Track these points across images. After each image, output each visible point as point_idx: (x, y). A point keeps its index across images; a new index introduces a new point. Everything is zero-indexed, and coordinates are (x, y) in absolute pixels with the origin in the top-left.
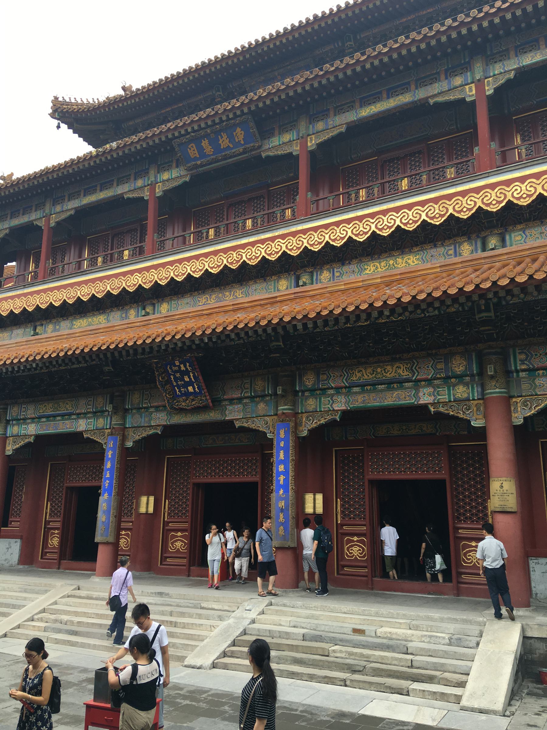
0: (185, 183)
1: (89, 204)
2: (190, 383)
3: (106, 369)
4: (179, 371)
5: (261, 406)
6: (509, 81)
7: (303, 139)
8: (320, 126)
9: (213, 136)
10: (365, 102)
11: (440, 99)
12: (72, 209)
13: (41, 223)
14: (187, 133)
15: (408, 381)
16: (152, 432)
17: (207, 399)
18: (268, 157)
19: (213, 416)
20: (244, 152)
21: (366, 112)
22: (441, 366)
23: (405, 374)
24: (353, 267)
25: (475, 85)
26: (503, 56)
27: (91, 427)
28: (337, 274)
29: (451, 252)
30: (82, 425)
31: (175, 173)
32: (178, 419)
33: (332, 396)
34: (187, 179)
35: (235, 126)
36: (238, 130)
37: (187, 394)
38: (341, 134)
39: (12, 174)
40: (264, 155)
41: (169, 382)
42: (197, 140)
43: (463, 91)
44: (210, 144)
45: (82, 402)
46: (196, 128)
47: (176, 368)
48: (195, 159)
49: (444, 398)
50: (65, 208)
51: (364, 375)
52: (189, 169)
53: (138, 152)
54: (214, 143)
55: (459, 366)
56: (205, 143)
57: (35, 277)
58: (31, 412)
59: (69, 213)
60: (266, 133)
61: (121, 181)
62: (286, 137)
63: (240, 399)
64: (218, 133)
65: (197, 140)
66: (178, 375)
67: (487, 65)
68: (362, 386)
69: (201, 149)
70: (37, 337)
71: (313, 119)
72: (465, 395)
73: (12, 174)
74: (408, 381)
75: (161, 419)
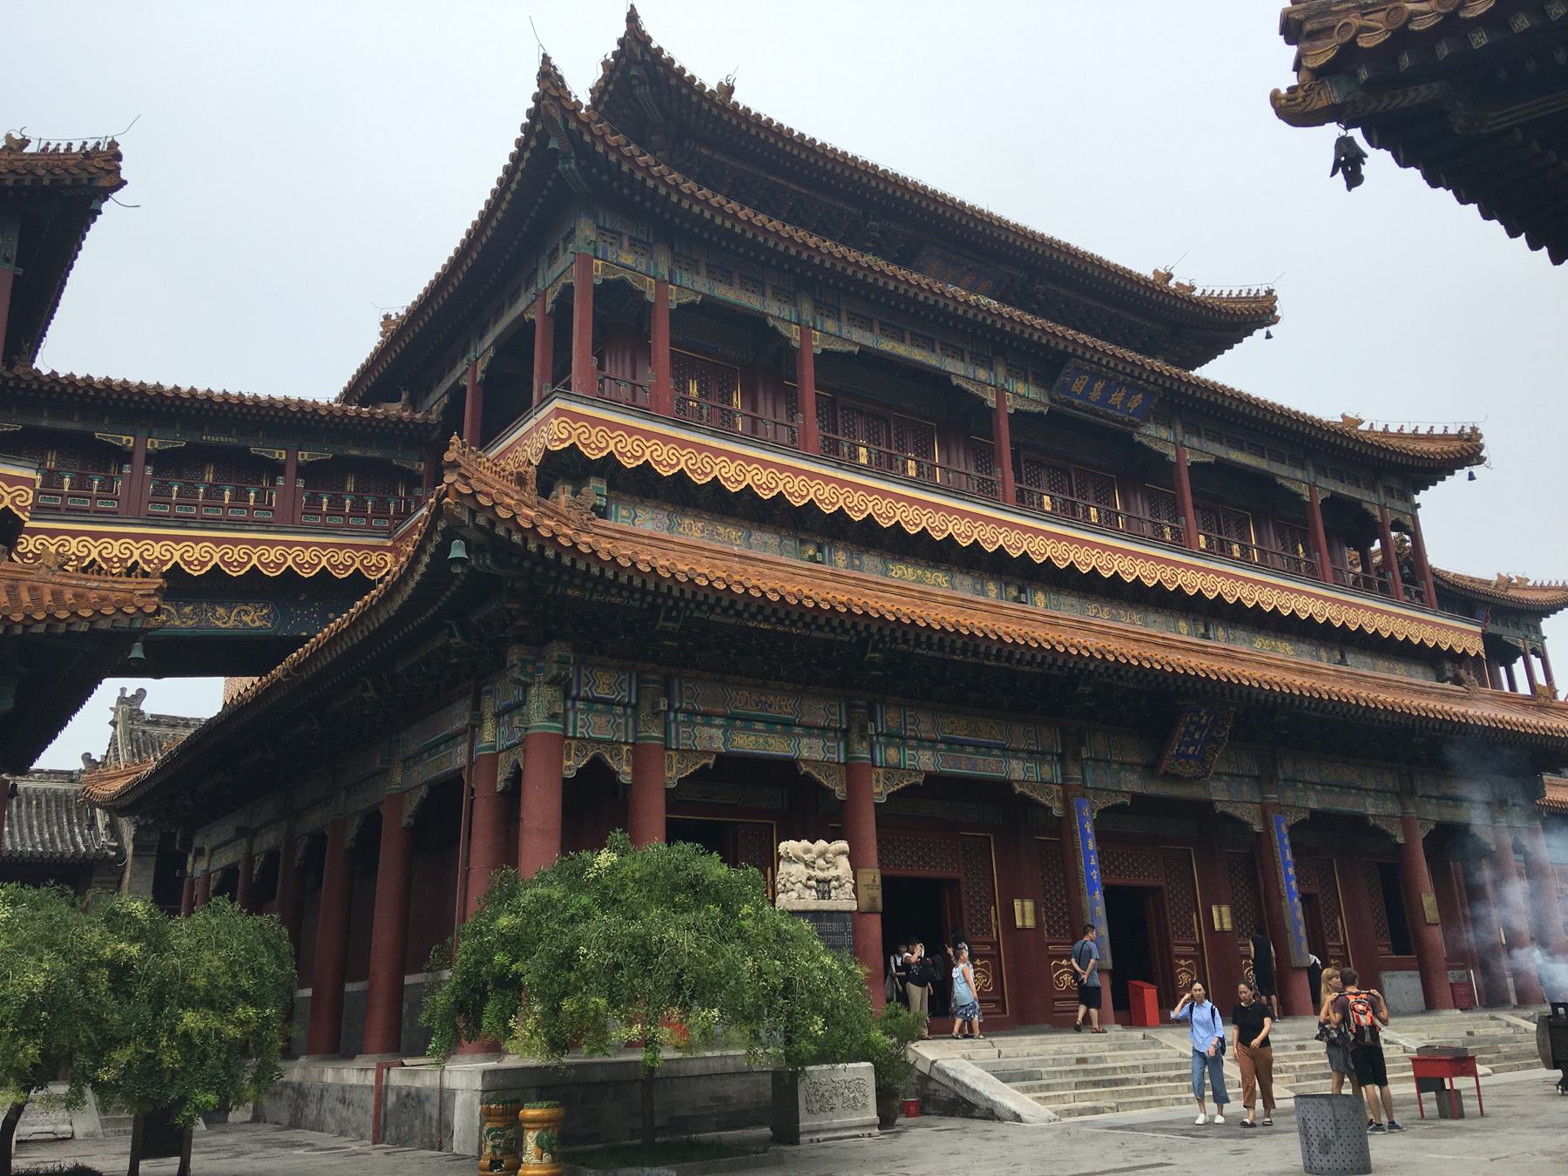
1: (890, 354)
12: (856, 344)
20: (1127, 424)
27: (1033, 776)
30: (1017, 770)
31: (1033, 392)
35: (1142, 389)
40: (1137, 438)
46: (1112, 365)
50: (845, 335)
53: (1038, 344)
54: (1108, 392)
56: (1099, 385)
59: (849, 348)
60: (1146, 415)
61: (958, 354)
62: (1164, 433)
64: (1120, 385)
65: (1095, 376)
69: (1089, 387)
70: (1205, 642)
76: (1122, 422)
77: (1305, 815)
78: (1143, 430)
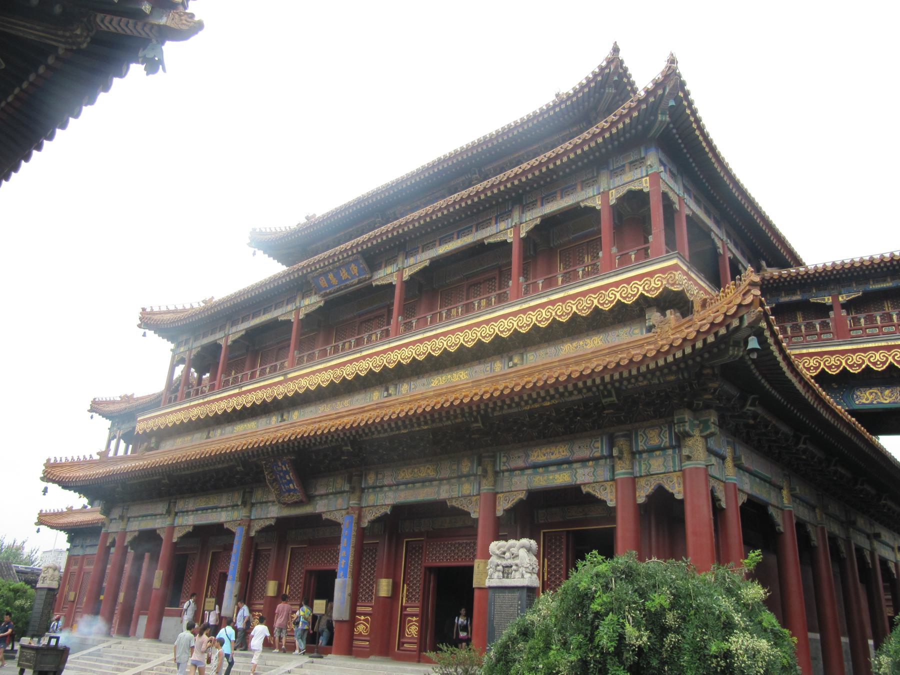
0: (320, 307)
2: (290, 482)
3: (238, 468)
4: (282, 471)
5: (340, 501)
6: (536, 226)
7: (401, 271)
8: (412, 261)
9: (335, 270)
10: (443, 241)
11: (492, 240)
13: (222, 342)
14: (316, 269)
15: (435, 480)
16: (268, 523)
17: (298, 496)
18: (377, 286)
19: (307, 510)
20: (358, 283)
21: (443, 250)
22: (455, 467)
23: (432, 474)
24: (424, 381)
25: (511, 230)
26: (532, 205)
27: (229, 519)
28: (413, 387)
29: (488, 369)
32: (287, 512)
33: (386, 492)
34: (322, 304)
35: (349, 263)
36: (353, 265)
37: (289, 491)
38: (426, 268)
39: (213, 298)
41: (275, 480)
42: (325, 274)
43: (506, 234)
44: (334, 276)
45: (225, 497)
47: (279, 469)
48: (326, 288)
49: (455, 494)
51: (405, 475)
52: (323, 296)
54: (337, 275)
55: (466, 467)
56: (331, 276)
57: (212, 388)
58: (191, 504)
63: (327, 495)
64: (339, 268)
66: (282, 474)
67: (523, 213)
68: (406, 484)
69: (329, 281)
71: (407, 255)
72: (468, 492)
73: (213, 298)
74: (435, 480)
75: (274, 512)
76: (365, 280)
77: (190, 529)
78: (375, 278)
